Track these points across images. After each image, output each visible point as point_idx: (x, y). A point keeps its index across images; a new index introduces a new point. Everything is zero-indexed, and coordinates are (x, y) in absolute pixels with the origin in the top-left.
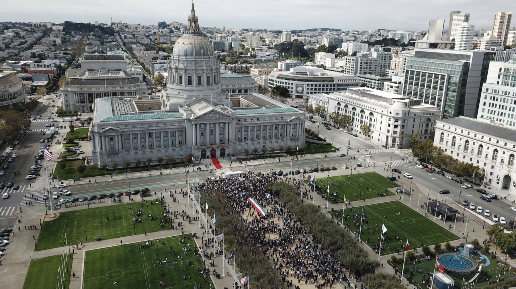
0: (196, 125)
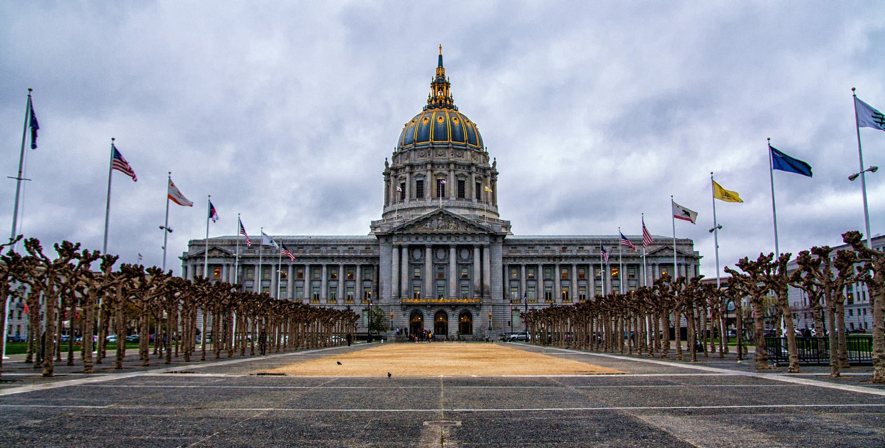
0: (400, 248)
